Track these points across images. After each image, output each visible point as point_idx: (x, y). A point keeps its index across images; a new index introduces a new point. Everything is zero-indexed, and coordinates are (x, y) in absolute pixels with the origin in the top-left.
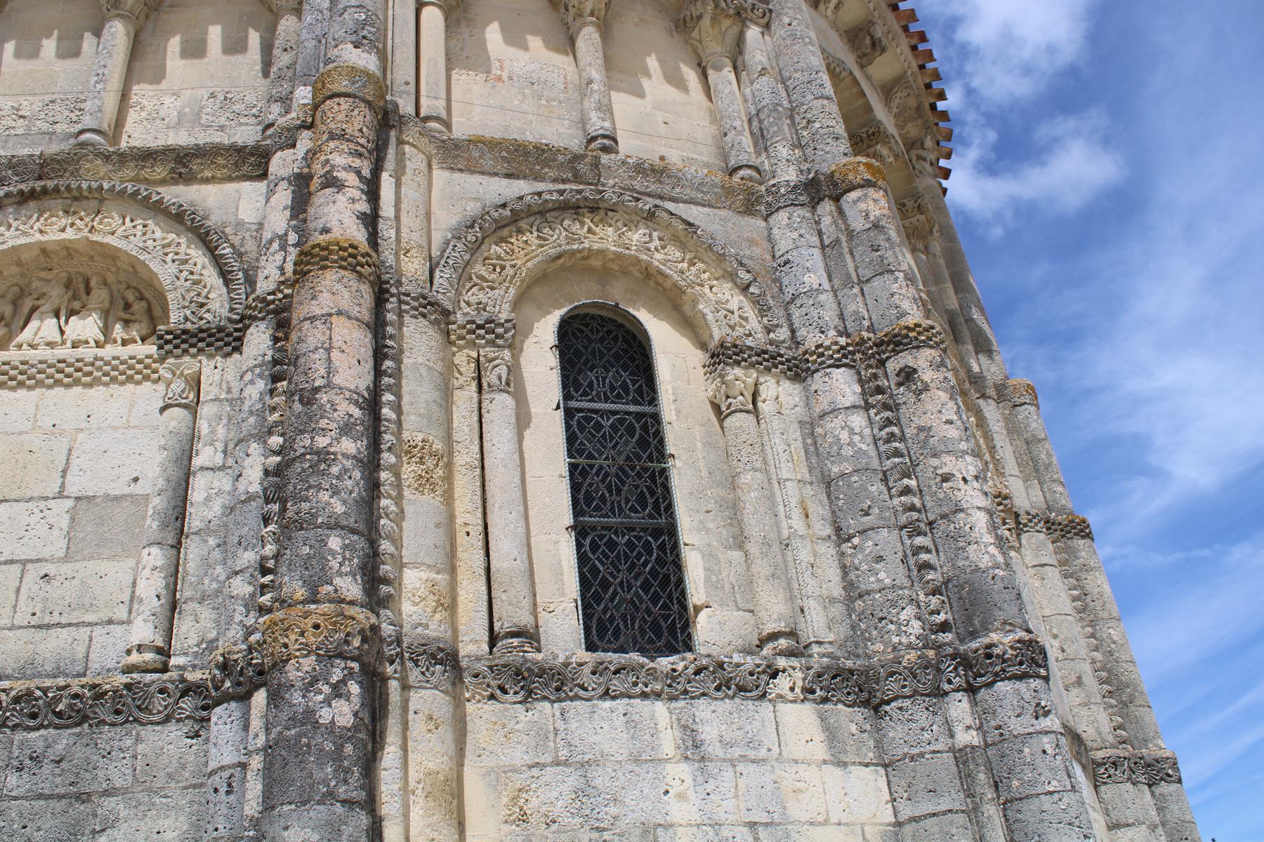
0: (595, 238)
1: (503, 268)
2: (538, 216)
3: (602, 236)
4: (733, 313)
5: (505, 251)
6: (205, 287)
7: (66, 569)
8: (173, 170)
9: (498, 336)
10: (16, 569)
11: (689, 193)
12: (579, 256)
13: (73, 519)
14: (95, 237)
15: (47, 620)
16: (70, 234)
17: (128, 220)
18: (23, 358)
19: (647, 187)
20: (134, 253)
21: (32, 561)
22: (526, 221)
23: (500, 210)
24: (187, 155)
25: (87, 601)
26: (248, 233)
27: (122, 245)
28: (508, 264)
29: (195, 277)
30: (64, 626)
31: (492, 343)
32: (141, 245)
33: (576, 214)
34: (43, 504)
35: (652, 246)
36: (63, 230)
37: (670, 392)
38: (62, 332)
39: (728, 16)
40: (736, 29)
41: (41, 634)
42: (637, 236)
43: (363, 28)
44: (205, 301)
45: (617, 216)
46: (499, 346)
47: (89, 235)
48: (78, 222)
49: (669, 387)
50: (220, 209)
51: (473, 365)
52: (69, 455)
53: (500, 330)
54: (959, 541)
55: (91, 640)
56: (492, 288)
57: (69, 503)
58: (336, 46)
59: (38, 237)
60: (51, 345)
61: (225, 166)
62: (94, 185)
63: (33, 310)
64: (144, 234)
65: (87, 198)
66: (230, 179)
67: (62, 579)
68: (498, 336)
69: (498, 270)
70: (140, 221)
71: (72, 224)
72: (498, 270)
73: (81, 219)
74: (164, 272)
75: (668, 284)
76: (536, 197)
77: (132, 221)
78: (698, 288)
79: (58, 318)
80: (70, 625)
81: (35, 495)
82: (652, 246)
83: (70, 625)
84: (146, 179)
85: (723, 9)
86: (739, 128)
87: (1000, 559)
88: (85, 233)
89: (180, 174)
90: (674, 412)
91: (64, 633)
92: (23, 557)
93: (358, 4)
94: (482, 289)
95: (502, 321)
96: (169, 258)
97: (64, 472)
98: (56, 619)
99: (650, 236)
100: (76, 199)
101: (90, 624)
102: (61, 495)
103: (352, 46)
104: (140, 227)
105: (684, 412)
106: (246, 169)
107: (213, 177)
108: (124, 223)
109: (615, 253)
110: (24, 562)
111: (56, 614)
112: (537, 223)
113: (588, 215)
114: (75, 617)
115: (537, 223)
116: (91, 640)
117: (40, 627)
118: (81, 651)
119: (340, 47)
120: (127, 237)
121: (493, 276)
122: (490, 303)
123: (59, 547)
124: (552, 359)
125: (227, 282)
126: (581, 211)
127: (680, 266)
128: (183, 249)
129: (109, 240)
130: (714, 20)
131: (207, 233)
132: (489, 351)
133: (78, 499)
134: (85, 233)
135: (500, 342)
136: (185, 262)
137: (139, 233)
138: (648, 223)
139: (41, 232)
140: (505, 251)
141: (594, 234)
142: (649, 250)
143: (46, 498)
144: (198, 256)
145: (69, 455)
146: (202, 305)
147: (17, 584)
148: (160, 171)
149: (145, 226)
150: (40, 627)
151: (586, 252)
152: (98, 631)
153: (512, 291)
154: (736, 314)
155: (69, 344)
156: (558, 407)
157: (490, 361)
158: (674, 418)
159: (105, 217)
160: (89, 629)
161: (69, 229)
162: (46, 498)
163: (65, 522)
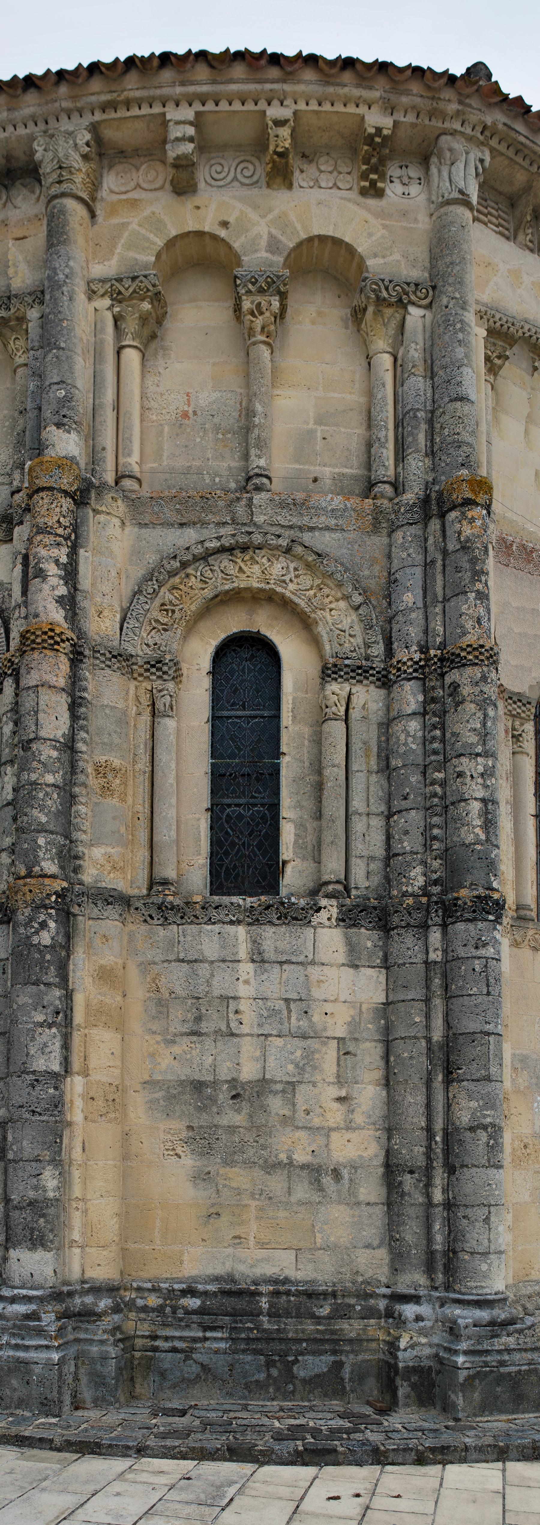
0: (243, 576)
1: (173, 612)
2: (201, 562)
3: (249, 574)
4: (344, 631)
5: (175, 597)
9: (165, 673)
11: (323, 520)
12: (232, 593)
19: (290, 521)
22: (193, 566)
23: (172, 562)
28: (177, 609)
31: (159, 677)
33: (232, 555)
35: (287, 578)
37: (290, 702)
39: (390, 305)
40: (398, 316)
42: (277, 568)
43: (64, 406)
45: (263, 552)
46: (165, 680)
49: (290, 698)
51: (148, 696)
53: (165, 668)
54: (461, 821)
56: (165, 630)
68: (165, 673)
69: (170, 614)
72: (170, 614)
75: (299, 610)
76: (199, 546)
78: (319, 612)
82: (287, 578)
85: (384, 299)
86: (383, 440)
87: (483, 837)
90: (290, 718)
94: (159, 631)
95: (167, 661)
99: (288, 568)
103: (55, 428)
105: (298, 717)
109: (258, 588)
112: (200, 568)
113: (239, 555)
115: (200, 568)
121: (166, 620)
122: (164, 644)
124: (206, 682)
126: (235, 552)
127: (308, 593)
130: (378, 313)
132: (158, 684)
135: (165, 677)
138: (287, 556)
140: (175, 597)
141: (244, 573)
142: (284, 581)
151: (237, 590)
153: (179, 631)
154: (347, 633)
156: (208, 721)
157: (160, 691)
158: (290, 722)
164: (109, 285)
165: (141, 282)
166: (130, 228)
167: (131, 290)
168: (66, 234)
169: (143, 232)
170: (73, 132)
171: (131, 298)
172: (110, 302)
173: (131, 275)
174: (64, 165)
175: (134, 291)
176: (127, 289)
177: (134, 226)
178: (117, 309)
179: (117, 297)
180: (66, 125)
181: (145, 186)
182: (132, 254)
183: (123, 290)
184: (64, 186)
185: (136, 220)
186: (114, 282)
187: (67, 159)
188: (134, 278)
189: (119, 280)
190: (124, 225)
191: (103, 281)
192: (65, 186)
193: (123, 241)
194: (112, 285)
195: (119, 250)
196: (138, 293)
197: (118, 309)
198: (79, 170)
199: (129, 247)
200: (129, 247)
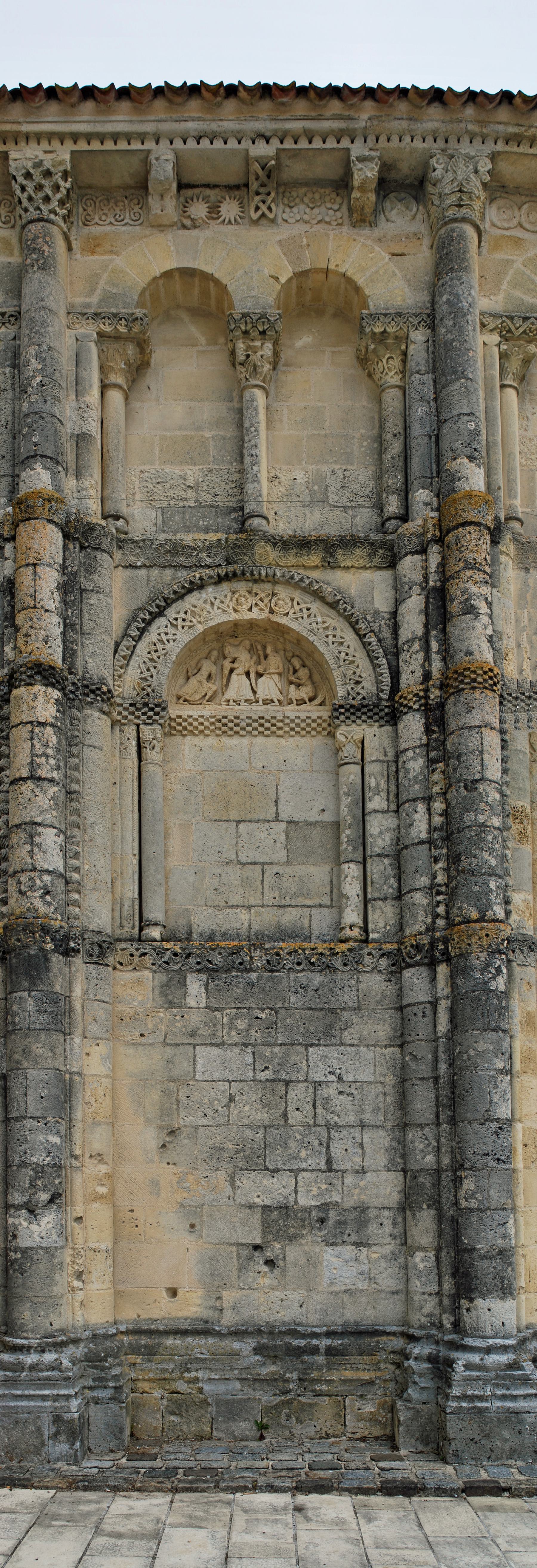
6: (358, 667)
7: (288, 870)
8: (324, 559)
10: (258, 868)
13: (287, 836)
14: (275, 618)
15: (283, 902)
16: (255, 614)
17: (295, 603)
18: (235, 714)
20: (304, 634)
21: (267, 864)
24: (333, 545)
25: (304, 891)
26: (383, 622)
27: (294, 626)
29: (351, 658)
30: (293, 907)
32: (309, 627)
34: (267, 825)
36: (250, 609)
41: (281, 911)
44: (359, 679)
47: (271, 616)
48: (259, 602)
50: (360, 597)
52: (277, 789)
55: (311, 916)
57: (283, 826)
58: (455, 459)
59: (234, 616)
61: (361, 557)
62: (271, 573)
64: (309, 616)
65: (263, 581)
66: (364, 568)
67: (287, 876)
70: (303, 606)
73: (262, 600)
74: (327, 651)
77: (298, 604)
80: (297, 906)
81: (261, 818)
83: (297, 906)
84: (304, 566)
88: (266, 614)
89: (329, 562)
91: (294, 911)
92: (261, 861)
93: (469, 411)
97: (276, 801)
98: (287, 902)
100: (256, 581)
101: (309, 907)
102: (277, 819)
104: (305, 610)
106: (377, 561)
107: (352, 567)
108: (293, 606)
110: (263, 864)
111: (287, 898)
114: (301, 901)
116: (311, 916)
117: (280, 906)
118: (306, 923)
119: (459, 461)
120: (297, 619)
123: (282, 855)
125: (375, 666)
129: (284, 621)
131: (357, 622)
133: (289, 822)
134: (266, 614)
137: (305, 616)
139: (235, 610)
143: (268, 821)
144: (350, 637)
145: (277, 789)
146: (357, 683)
147: (261, 878)
148: (314, 559)
149: (308, 609)
150: (280, 906)
152: (314, 911)
159: (279, 599)
160: (309, 909)
161: (255, 609)
162: (268, 821)
163: (283, 837)
164: (500, 321)
165: (533, 324)
166: (515, 266)
167: (521, 330)
168: (467, 261)
169: (528, 272)
170: (473, 157)
171: (519, 338)
172: (499, 339)
173: (523, 315)
174: (465, 190)
175: (524, 332)
176: (517, 329)
177: (518, 265)
178: (504, 347)
179: (506, 335)
180: (465, 148)
181: (527, 226)
182: (518, 293)
183: (513, 329)
184: (464, 210)
185: (521, 260)
186: (504, 319)
187: (468, 184)
188: (525, 319)
189: (511, 318)
190: (509, 263)
191: (495, 316)
192: (465, 211)
193: (508, 278)
194: (503, 322)
195: (504, 286)
196: (527, 334)
197: (505, 347)
198: (478, 197)
199: (515, 285)
200: (515, 285)
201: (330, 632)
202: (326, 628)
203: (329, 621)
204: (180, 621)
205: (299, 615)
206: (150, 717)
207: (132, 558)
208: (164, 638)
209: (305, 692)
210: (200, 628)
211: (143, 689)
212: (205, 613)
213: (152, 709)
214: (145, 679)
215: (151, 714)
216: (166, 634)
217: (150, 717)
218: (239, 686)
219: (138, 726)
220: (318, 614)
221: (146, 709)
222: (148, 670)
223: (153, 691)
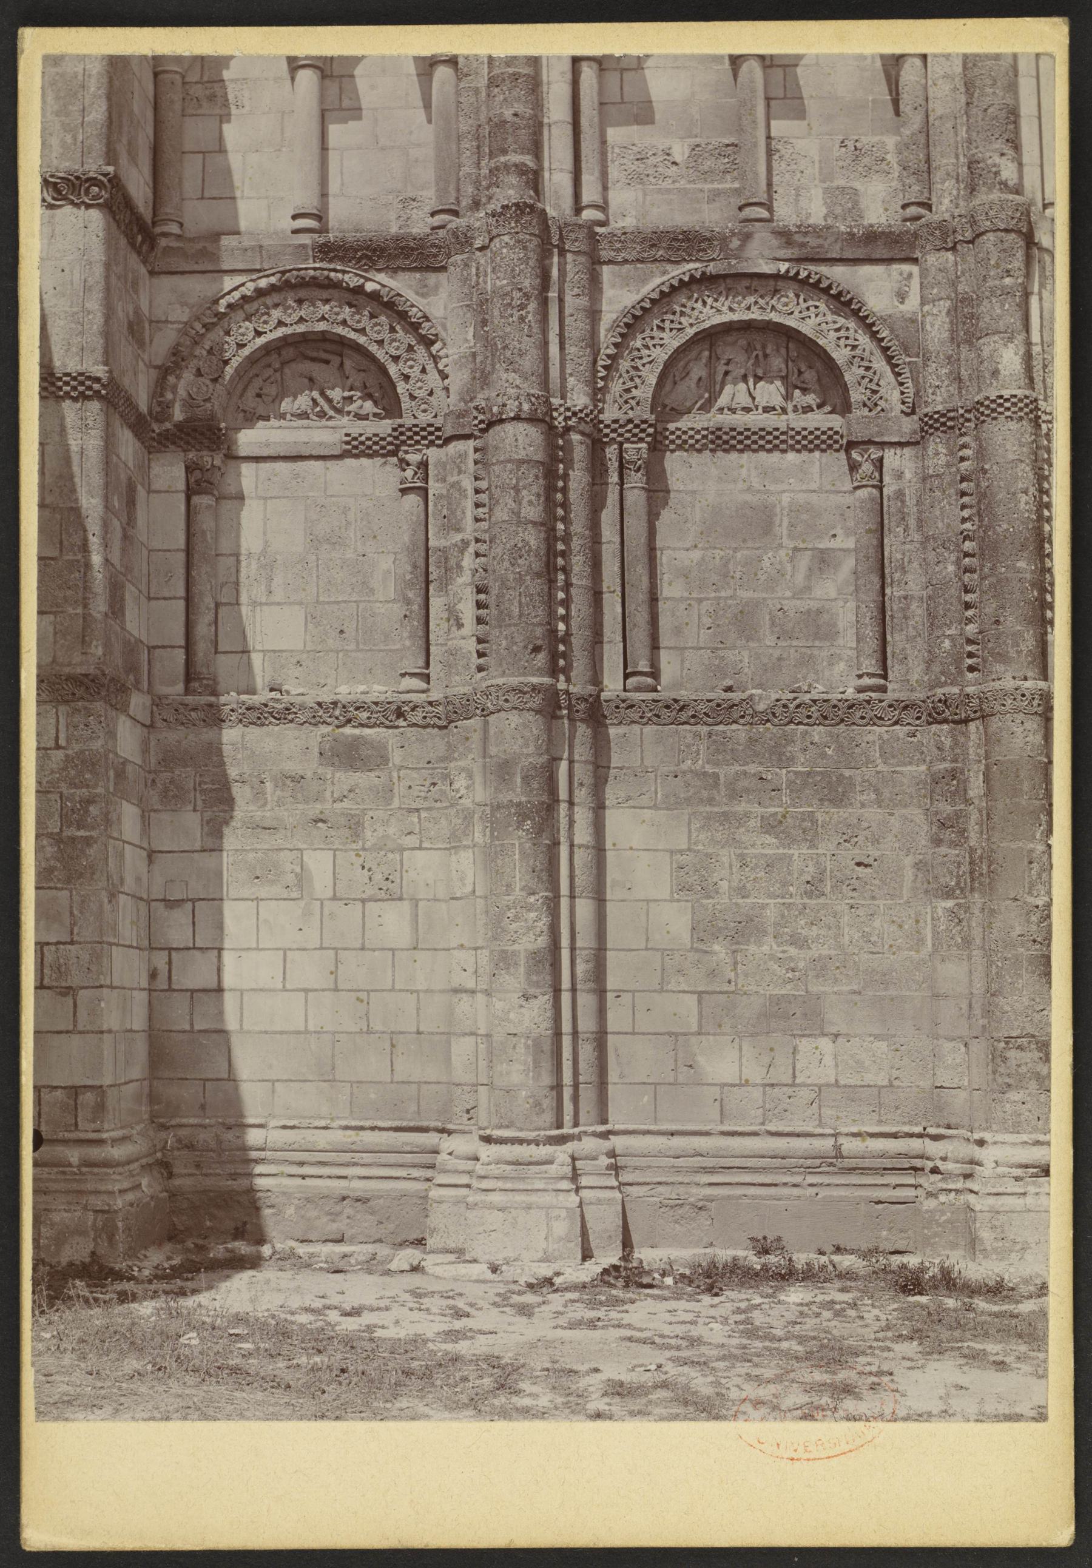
17: (801, 300)
36: (749, 308)
38: (754, 399)
60: (747, 410)
63: (726, 373)
71: (756, 303)
74: (840, 355)
79: (746, 383)
96: (842, 342)
128: (851, 333)
136: (854, 347)
139: (731, 309)
155: (760, 410)
201: (842, 333)
202: (838, 330)
203: (841, 321)
204: (667, 324)
205: (805, 314)
206: (635, 435)
207: (613, 254)
208: (650, 343)
209: (811, 399)
210: (691, 332)
211: (626, 402)
212: (696, 313)
213: (637, 426)
214: (628, 391)
215: (636, 431)
216: (652, 338)
217: (635, 435)
218: (734, 393)
219: (621, 444)
220: (828, 313)
221: (630, 426)
222: (632, 379)
223: (638, 404)
